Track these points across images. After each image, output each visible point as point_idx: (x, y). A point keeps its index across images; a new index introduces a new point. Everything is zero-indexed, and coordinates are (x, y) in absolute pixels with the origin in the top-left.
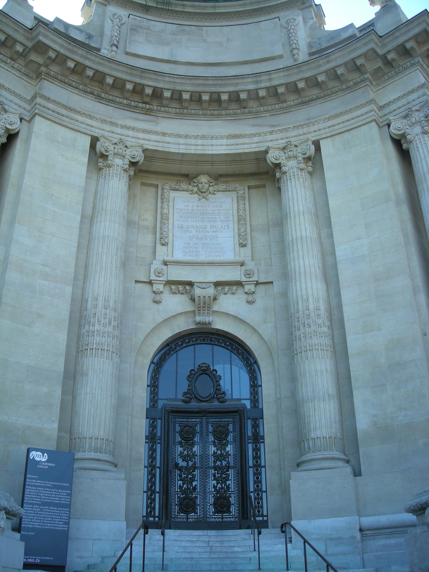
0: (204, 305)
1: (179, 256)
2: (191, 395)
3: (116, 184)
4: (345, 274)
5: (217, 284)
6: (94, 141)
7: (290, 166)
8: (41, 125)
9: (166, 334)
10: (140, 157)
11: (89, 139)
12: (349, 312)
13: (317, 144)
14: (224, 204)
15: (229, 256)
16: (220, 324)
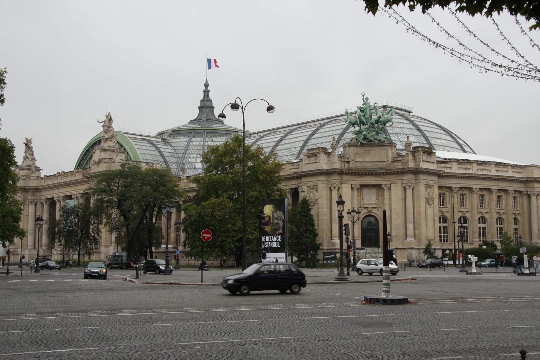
0: (370, 211)
1: (366, 203)
2: (368, 226)
3: (355, 193)
4: (393, 211)
5: (373, 208)
6: (351, 185)
7: (386, 188)
8: (343, 185)
9: (364, 216)
10: (359, 187)
11: (350, 185)
12: (393, 217)
13: (391, 184)
14: (373, 191)
15: (374, 203)
16: (373, 214)
